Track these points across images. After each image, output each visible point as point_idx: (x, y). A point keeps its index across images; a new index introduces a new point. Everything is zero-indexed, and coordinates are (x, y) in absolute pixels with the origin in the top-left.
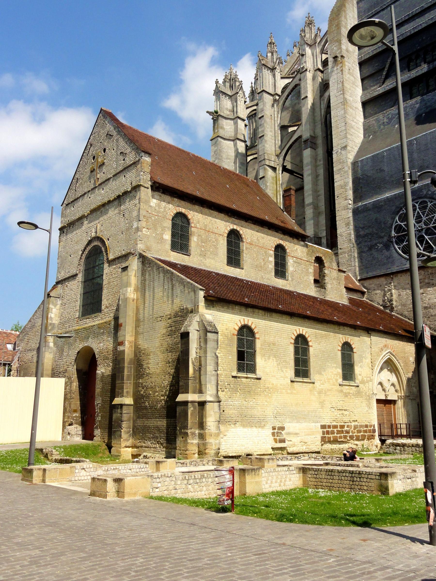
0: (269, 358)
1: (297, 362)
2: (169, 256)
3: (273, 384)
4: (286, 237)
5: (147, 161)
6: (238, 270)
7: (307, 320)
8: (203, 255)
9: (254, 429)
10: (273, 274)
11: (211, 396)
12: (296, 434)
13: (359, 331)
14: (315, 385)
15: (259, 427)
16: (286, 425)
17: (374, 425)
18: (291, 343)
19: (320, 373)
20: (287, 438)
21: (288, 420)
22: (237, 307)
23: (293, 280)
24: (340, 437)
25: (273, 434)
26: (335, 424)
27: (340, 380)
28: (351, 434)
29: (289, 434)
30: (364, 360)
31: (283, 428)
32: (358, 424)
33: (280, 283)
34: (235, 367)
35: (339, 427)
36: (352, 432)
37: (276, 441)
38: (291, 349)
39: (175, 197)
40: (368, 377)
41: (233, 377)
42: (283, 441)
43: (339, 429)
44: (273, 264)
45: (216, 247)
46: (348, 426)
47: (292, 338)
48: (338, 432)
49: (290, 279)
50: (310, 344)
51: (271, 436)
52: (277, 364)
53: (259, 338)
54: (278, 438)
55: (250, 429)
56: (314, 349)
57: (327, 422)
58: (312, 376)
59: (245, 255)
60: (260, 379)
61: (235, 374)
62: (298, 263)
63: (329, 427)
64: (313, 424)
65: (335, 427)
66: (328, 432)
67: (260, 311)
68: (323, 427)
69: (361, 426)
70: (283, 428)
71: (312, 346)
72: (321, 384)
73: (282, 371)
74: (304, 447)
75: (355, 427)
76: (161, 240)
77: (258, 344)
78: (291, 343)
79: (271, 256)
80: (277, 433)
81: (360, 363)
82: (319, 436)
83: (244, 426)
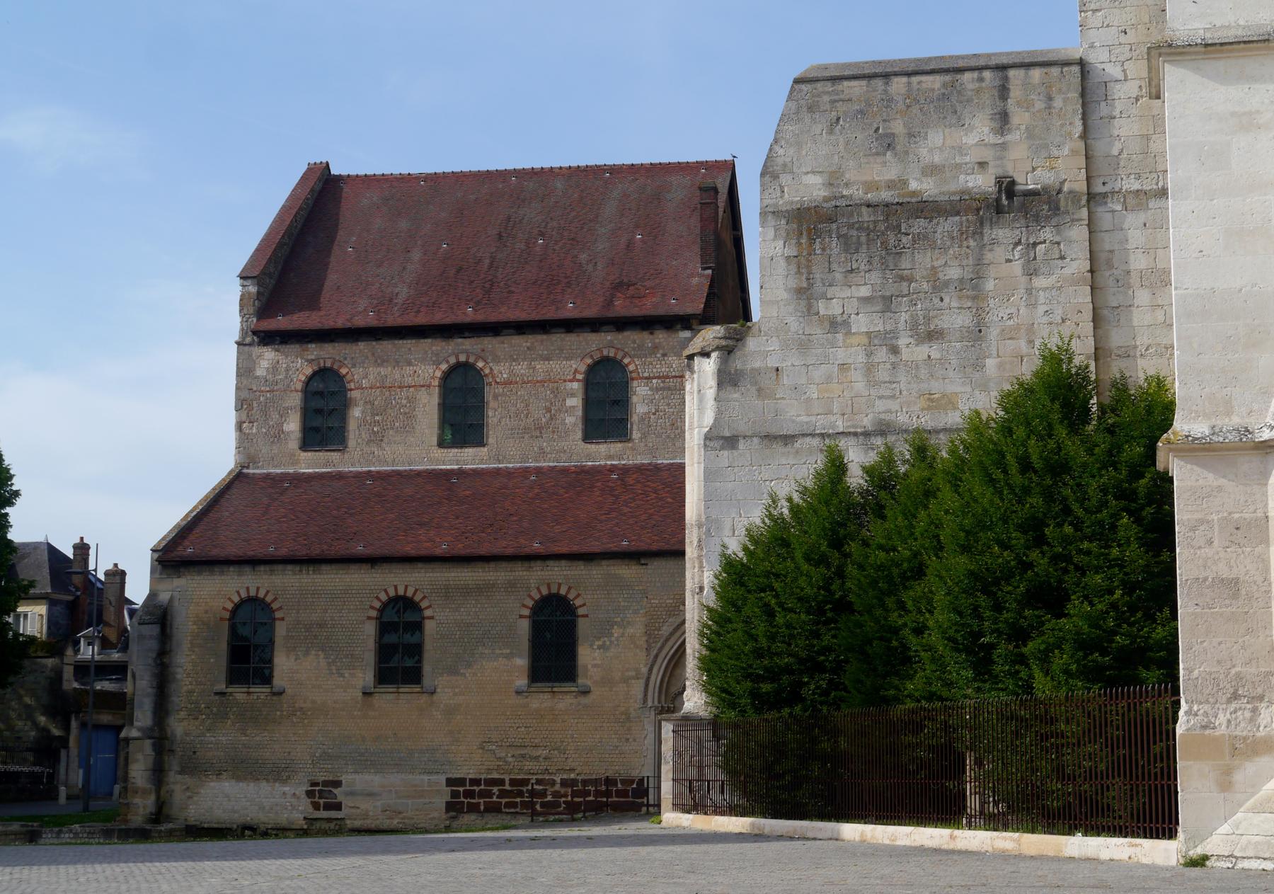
0: (307, 653)
1: (384, 652)
2: (296, 462)
3: (313, 702)
4: (626, 334)
5: (249, 293)
6: (469, 452)
7: (420, 565)
8: (377, 439)
9: (264, 784)
10: (579, 435)
11: (139, 729)
12: (371, 795)
13: (604, 563)
14: (435, 697)
15: (275, 781)
16: (344, 778)
17: (642, 780)
18: (369, 618)
19: (453, 671)
20: (346, 802)
21: (351, 769)
22: (231, 569)
23: (644, 436)
24: (514, 805)
25: (310, 794)
26: (495, 776)
27: (522, 682)
28: (549, 798)
29: (352, 794)
30: (616, 632)
31: (337, 784)
32: (580, 778)
33: (604, 454)
34: (223, 676)
35: (507, 782)
36: (555, 794)
37: (316, 806)
38: (370, 629)
39: (310, 342)
40: (628, 670)
41: (216, 694)
42: (338, 807)
43: (507, 787)
44: (580, 413)
45: (409, 416)
46: (539, 782)
47: (372, 607)
48: (503, 794)
49: (636, 435)
50: (427, 613)
51: (304, 796)
52: (329, 664)
53: (283, 619)
54: (322, 801)
55: (252, 784)
56: (437, 624)
57: (468, 772)
58: (427, 681)
59: (490, 414)
60: (280, 693)
61: (222, 687)
62: (669, 389)
63: (475, 782)
64: (426, 777)
65: (502, 782)
66: (468, 794)
67: (290, 567)
68: (450, 782)
69: (585, 782)
70: (337, 784)
71: (432, 618)
72: (455, 694)
73: (342, 675)
74: (395, 822)
75: (564, 783)
76: (278, 435)
77: (281, 630)
78: (369, 618)
79: (573, 395)
80: (320, 791)
81: (599, 639)
82: (441, 801)
83: (239, 779)
